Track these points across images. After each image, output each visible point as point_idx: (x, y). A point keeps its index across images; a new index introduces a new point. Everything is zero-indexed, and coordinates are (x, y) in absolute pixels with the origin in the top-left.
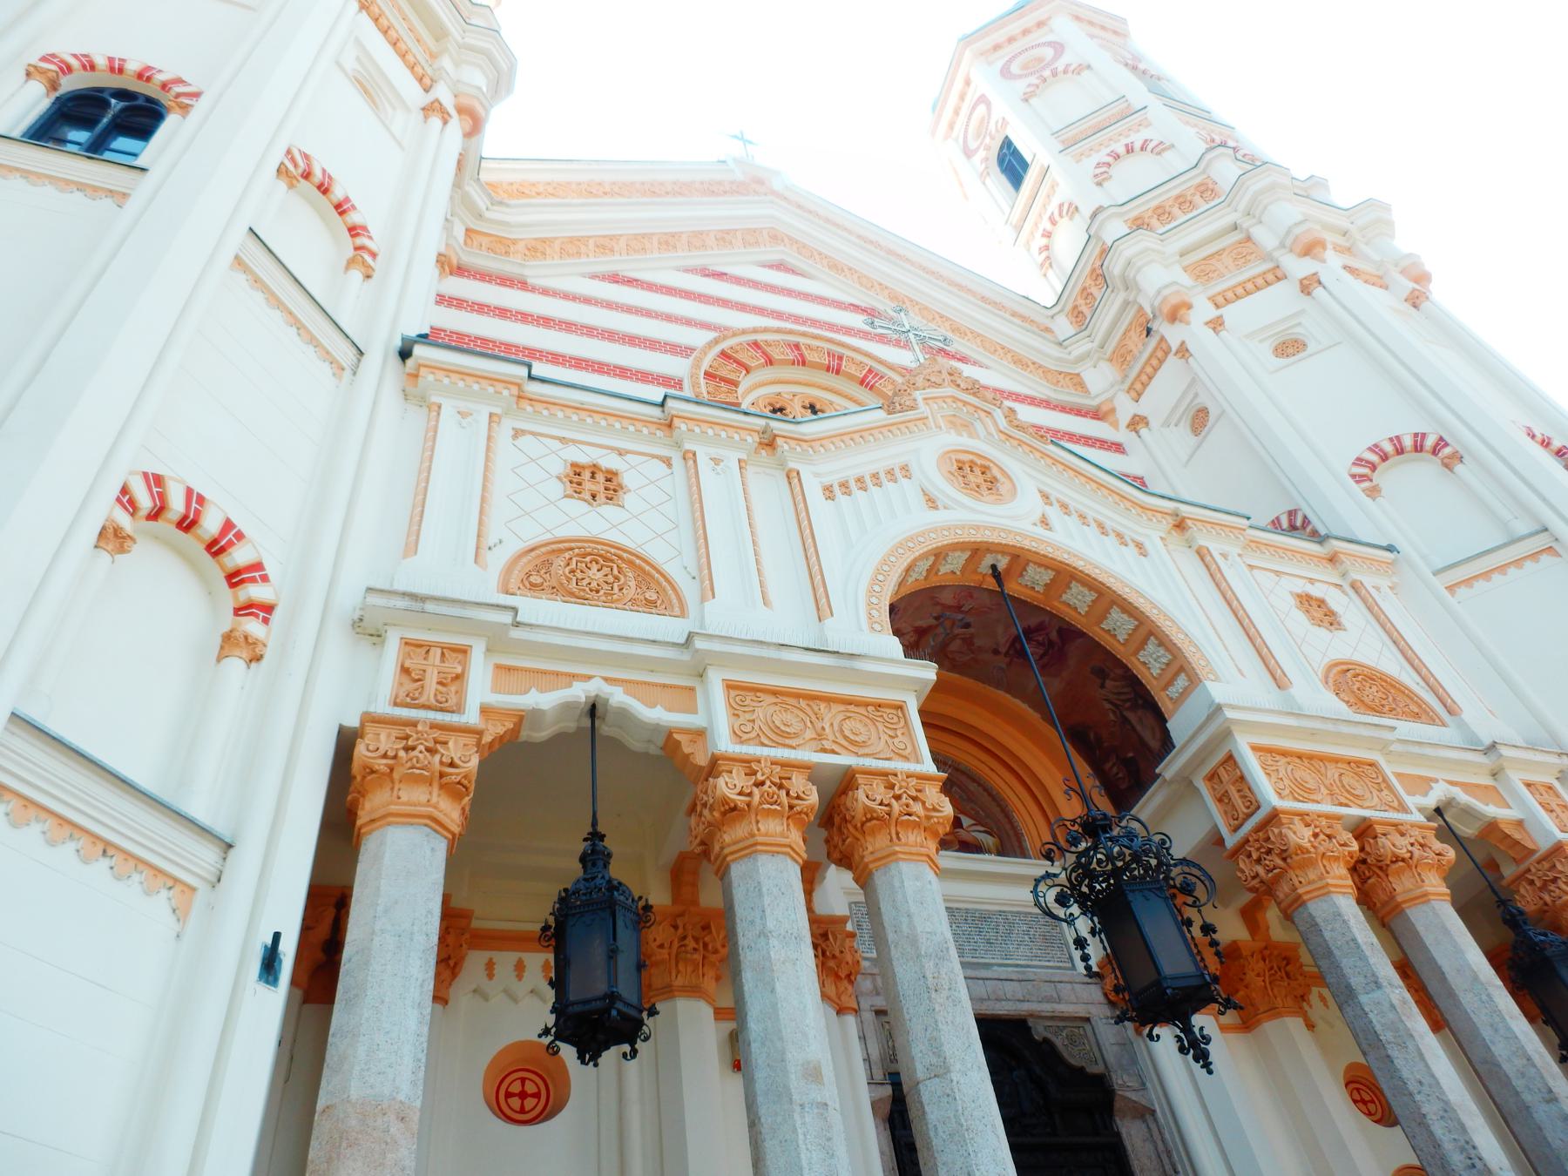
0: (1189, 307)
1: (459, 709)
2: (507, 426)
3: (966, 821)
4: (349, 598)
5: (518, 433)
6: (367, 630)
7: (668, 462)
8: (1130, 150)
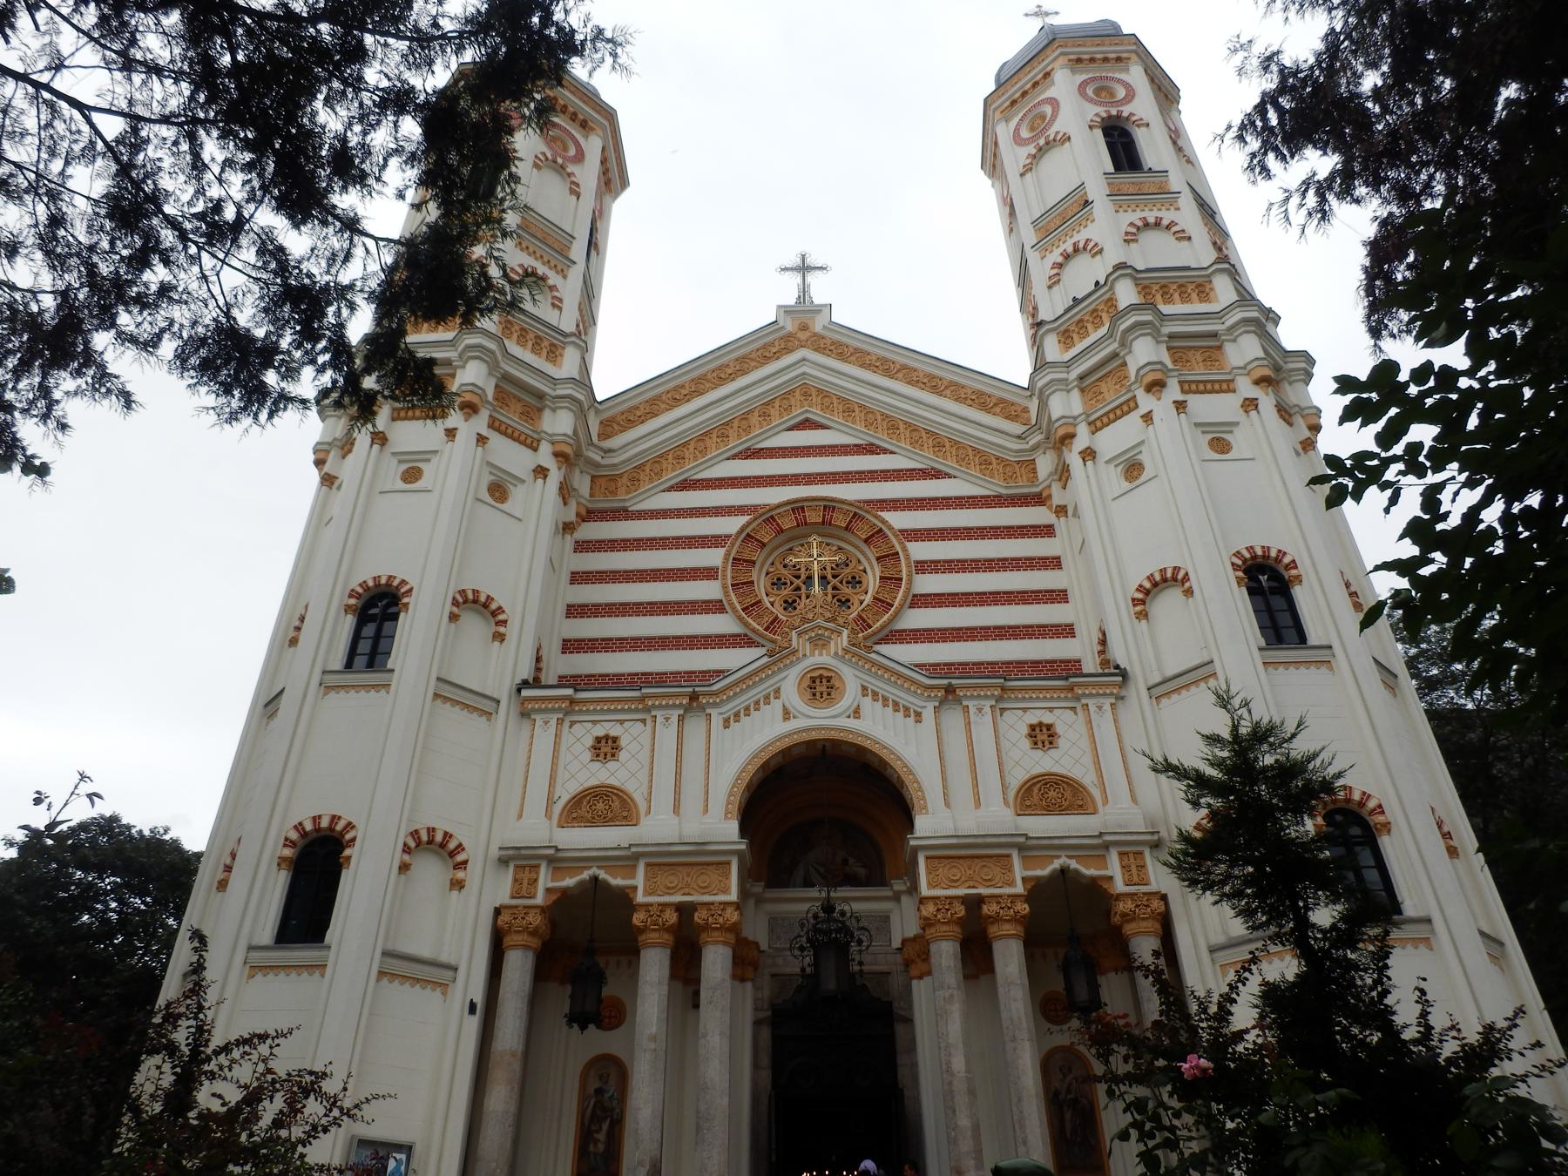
0: (1073, 436)
1: (533, 897)
2: (566, 724)
3: (851, 861)
4: (494, 852)
5: (572, 723)
6: (503, 862)
7: (644, 721)
8: (1076, 250)
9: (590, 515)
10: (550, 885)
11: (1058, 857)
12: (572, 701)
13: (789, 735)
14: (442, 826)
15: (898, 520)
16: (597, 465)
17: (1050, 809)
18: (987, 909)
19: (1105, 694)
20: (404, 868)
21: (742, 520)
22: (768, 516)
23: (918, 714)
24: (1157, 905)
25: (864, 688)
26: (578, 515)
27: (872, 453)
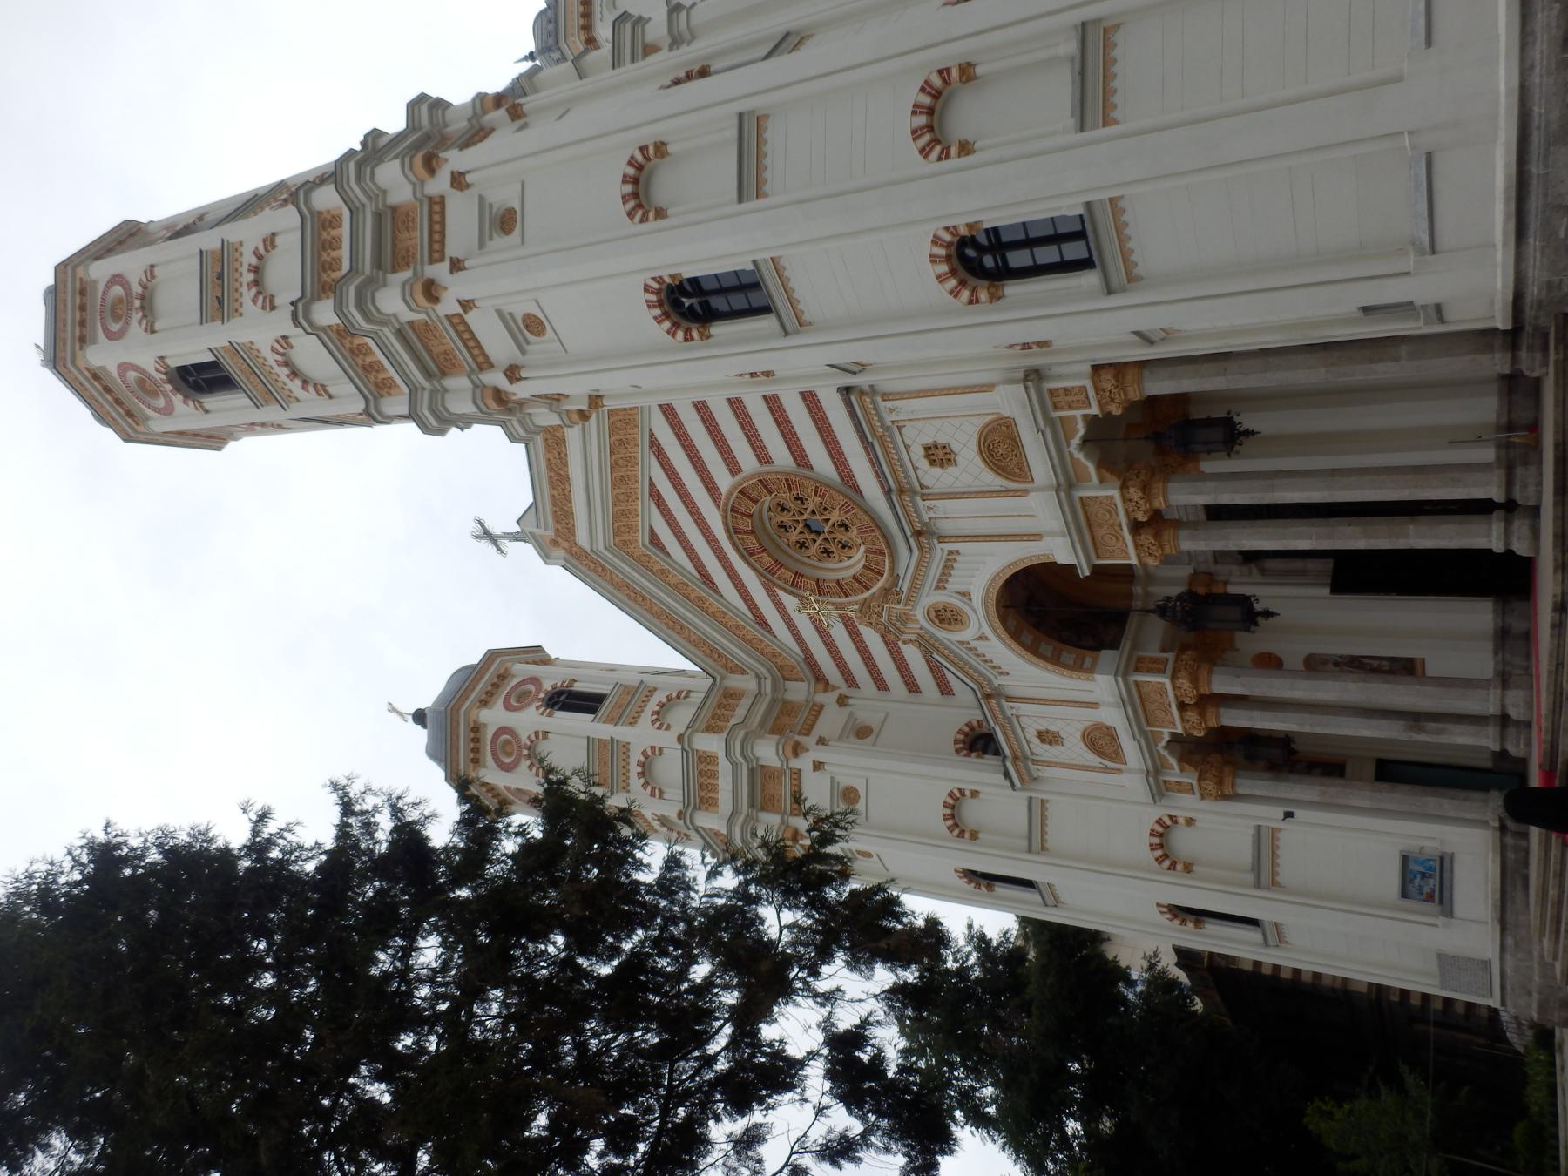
9: (819, 677)
10: (1177, 770)
11: (1071, 455)
12: (1016, 758)
13: (1004, 642)
14: (1147, 840)
15: (724, 481)
16: (774, 679)
17: (1015, 443)
18: (1142, 517)
19: (875, 408)
20: (1188, 868)
21: (782, 594)
22: (768, 577)
23: (950, 552)
24: (1108, 381)
25: (937, 588)
26: (825, 690)
27: (659, 495)
